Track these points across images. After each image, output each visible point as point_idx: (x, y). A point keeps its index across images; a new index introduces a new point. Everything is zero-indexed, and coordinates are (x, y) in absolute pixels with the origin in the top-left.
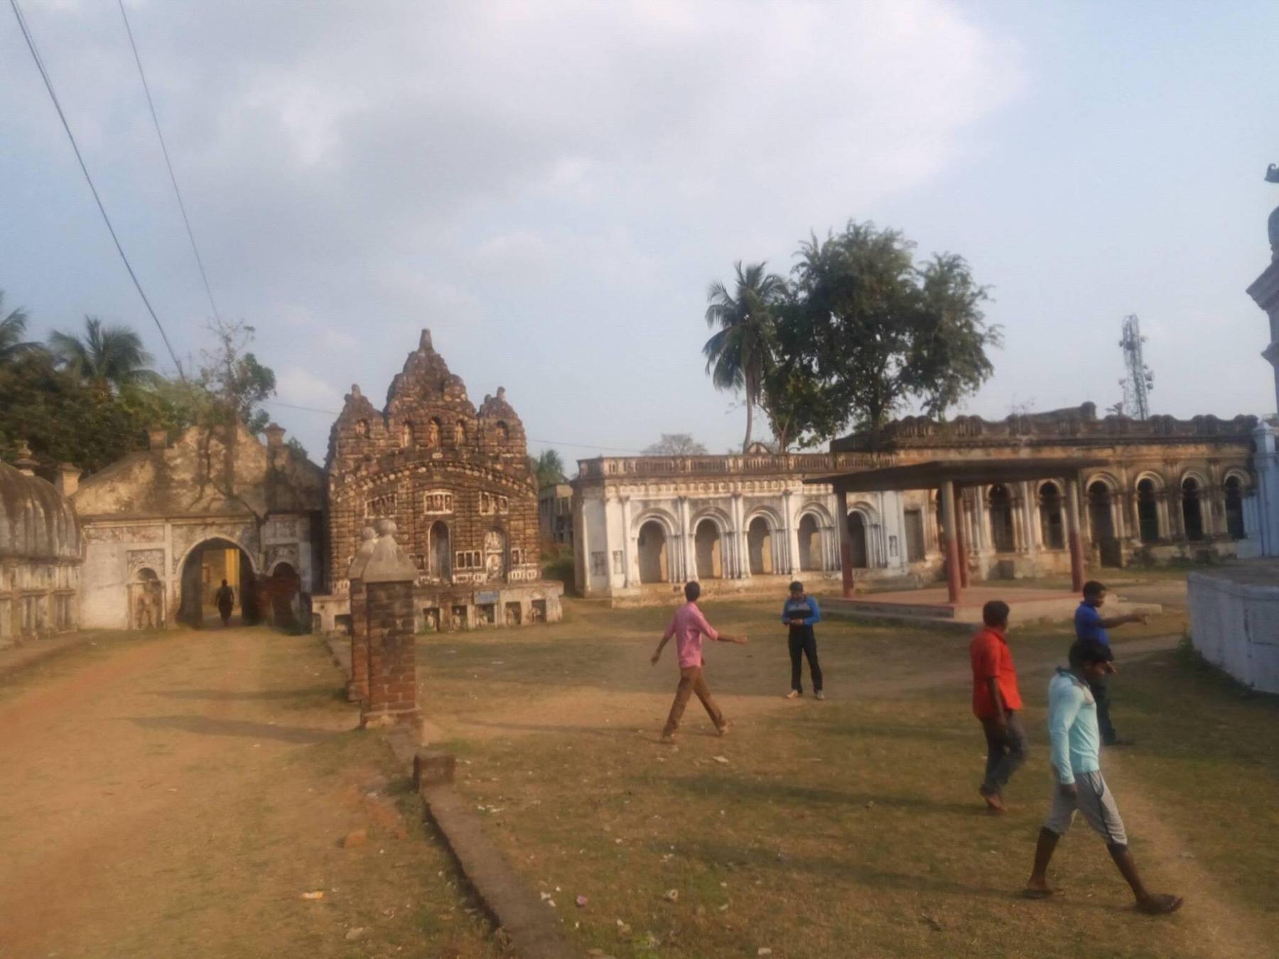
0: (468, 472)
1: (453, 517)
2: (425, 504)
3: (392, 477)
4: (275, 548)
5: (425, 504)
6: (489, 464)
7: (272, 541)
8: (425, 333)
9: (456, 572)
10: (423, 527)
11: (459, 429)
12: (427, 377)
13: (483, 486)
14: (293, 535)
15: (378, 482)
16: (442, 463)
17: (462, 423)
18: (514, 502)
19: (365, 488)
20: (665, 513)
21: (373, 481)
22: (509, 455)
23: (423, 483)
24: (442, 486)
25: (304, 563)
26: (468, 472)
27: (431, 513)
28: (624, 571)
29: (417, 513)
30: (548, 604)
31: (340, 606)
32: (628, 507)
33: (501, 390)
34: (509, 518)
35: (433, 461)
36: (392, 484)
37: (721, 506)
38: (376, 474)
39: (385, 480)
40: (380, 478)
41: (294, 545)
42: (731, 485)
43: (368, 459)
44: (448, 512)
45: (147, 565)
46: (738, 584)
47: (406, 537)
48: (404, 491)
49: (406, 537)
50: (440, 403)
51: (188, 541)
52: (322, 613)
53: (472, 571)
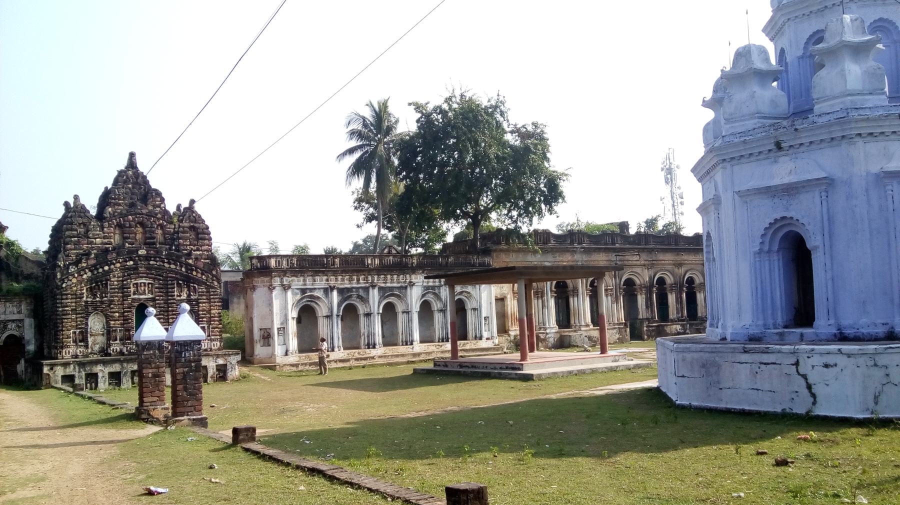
0: (166, 265)
1: (153, 300)
2: (132, 289)
3: (106, 268)
5: (132, 289)
8: (132, 155)
11: (159, 232)
12: (132, 190)
13: (178, 276)
14: (19, 312)
16: (147, 258)
18: (203, 289)
19: (85, 276)
20: (318, 298)
21: (90, 271)
25: (29, 333)
26: (166, 265)
27: (136, 296)
28: (285, 343)
29: (125, 296)
30: (229, 367)
31: (65, 368)
32: (289, 293)
33: (192, 202)
35: (139, 256)
37: (361, 293)
38: (94, 266)
39: (101, 270)
40: (97, 269)
41: (21, 321)
42: (370, 278)
43: (87, 254)
44: (150, 296)
46: (373, 352)
50: (144, 211)
52: (51, 373)
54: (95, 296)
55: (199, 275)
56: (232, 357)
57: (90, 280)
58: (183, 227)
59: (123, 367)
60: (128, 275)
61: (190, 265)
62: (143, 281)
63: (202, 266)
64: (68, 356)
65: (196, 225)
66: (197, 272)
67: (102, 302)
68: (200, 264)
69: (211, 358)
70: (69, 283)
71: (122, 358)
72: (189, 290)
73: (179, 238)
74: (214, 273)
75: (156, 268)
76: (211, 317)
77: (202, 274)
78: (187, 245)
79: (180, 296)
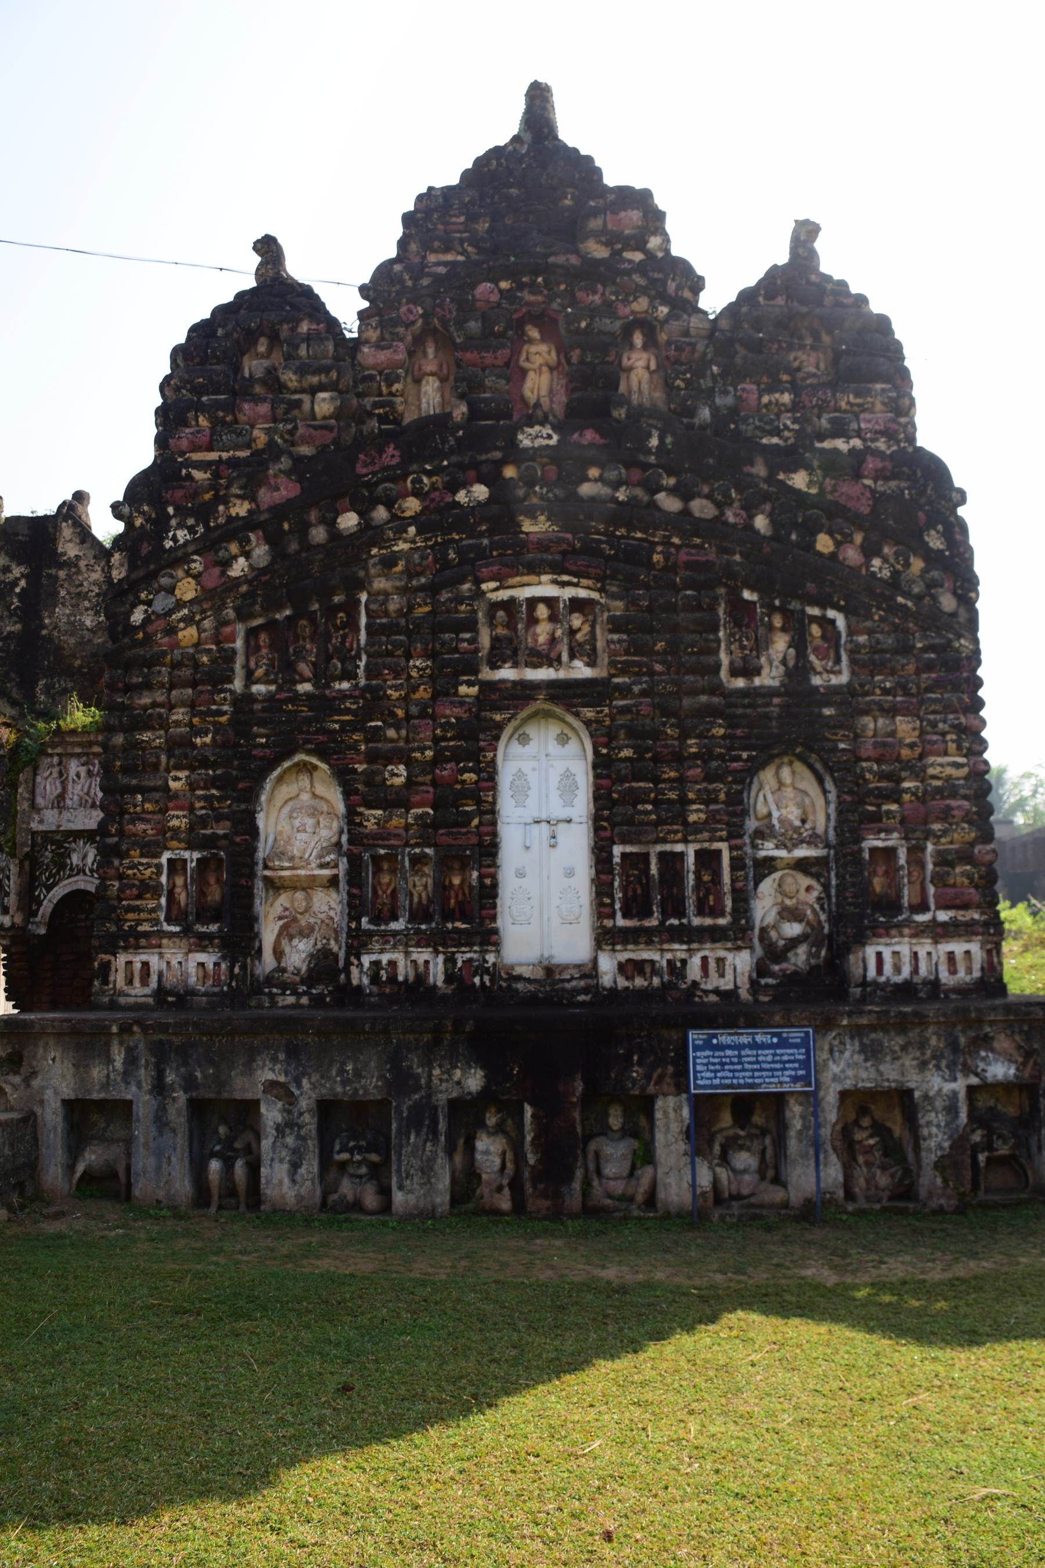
0: (670, 504)
2: (485, 641)
3: (349, 521)
4: (62, 841)
6: (760, 469)
7: (50, 820)
8: (538, 98)
12: (529, 227)
17: (648, 326)
19: (239, 567)
22: (841, 444)
24: (558, 561)
26: (670, 504)
27: (507, 673)
33: (805, 235)
34: (848, 700)
39: (319, 534)
40: (303, 529)
44: (581, 670)
47: (398, 775)
49: (398, 775)
55: (852, 555)
60: (463, 560)
62: (544, 588)
67: (324, 704)
68: (855, 494)
70: (162, 602)
72: (799, 643)
74: (935, 541)
76: (922, 798)
77: (870, 550)
79: (749, 671)
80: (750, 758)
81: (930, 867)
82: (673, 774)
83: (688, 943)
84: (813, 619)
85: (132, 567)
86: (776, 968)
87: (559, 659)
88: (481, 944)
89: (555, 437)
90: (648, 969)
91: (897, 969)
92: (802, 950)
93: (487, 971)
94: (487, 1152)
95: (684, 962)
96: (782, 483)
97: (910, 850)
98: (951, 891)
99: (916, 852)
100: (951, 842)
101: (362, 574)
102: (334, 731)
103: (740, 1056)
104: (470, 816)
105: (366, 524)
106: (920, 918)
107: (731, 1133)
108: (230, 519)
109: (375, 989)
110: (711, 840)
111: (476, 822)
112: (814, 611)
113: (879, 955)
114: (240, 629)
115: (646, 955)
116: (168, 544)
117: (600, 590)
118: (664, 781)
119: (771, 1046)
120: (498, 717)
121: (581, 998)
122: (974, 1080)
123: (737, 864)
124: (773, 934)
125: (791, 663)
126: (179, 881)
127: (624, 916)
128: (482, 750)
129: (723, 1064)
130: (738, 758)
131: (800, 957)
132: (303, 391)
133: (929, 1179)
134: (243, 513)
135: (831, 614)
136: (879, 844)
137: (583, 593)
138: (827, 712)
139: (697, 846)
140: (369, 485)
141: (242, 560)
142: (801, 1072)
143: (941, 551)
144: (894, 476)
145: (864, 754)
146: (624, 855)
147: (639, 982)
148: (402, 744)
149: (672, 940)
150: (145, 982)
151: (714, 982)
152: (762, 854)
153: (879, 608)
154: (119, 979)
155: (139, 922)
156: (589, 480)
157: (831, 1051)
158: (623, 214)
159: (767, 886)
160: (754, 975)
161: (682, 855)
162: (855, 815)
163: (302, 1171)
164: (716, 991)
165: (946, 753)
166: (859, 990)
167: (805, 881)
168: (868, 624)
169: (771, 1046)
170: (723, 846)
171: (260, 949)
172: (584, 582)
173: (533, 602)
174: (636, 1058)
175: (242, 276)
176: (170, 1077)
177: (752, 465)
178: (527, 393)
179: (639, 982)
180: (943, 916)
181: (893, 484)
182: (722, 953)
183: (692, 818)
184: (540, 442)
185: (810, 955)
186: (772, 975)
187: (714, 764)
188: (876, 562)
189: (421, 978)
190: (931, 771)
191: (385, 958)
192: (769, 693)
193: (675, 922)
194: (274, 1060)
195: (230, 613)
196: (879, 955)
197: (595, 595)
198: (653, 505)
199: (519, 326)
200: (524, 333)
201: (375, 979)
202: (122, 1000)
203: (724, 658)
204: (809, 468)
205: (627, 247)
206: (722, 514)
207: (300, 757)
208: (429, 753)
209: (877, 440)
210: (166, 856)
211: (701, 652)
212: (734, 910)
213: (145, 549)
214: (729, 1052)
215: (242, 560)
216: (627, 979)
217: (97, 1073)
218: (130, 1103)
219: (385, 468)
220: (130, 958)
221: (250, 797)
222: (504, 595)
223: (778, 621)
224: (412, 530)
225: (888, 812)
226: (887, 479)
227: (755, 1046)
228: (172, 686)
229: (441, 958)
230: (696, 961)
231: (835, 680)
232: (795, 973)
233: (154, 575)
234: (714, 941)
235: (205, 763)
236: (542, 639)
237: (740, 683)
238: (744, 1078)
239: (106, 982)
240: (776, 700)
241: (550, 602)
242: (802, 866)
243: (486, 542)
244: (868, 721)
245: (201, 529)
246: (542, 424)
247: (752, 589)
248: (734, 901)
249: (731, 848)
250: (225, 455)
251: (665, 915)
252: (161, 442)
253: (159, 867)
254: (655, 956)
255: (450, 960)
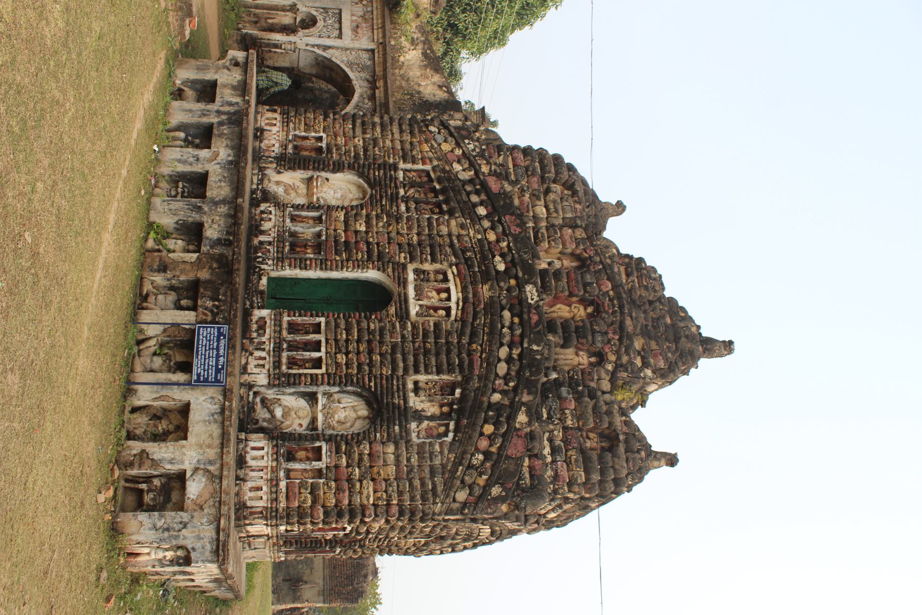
0: (503, 352)
1: (403, 315)
2: (427, 266)
8: (728, 347)
9: (278, 323)
10: (381, 260)
13: (475, 383)
15: (469, 188)
19: (457, 167)
23: (475, 266)
26: (503, 352)
27: (411, 276)
30: (171, 517)
31: (234, 88)
33: (672, 460)
35: (520, 286)
36: (469, 210)
38: (485, 187)
39: (475, 199)
40: (477, 193)
44: (414, 310)
45: (320, 24)
48: (455, 230)
51: (350, 65)
53: (278, 349)
54: (413, 185)
55: (483, 444)
56: (209, 532)
57: (448, 178)
58: (609, 413)
59: (216, 203)
61: (511, 418)
63: (511, 451)
64: (262, 123)
65: (622, 448)
66: (491, 438)
67: (394, 198)
68: (516, 447)
69: (212, 453)
70: (440, 138)
71: (245, 201)
72: (432, 418)
73: (578, 398)
74: (496, 491)
75: (492, 325)
77: (487, 454)
78: (562, 420)
79: (417, 389)
80: (370, 387)
81: (311, 481)
82: (361, 349)
83: (274, 351)
84: (447, 426)
85: (456, 128)
86: (258, 400)
87: (419, 300)
88: (278, 258)
89: (532, 302)
90: (261, 332)
91: (254, 458)
92: (268, 416)
93: (264, 260)
94: (176, 243)
95: (264, 350)
96: (520, 409)
97: (320, 470)
98: (297, 490)
99: (319, 473)
100: (324, 493)
101: (457, 215)
102: (381, 202)
103: (213, 349)
104: (340, 255)
105: (480, 218)
106: (282, 474)
107: (173, 358)
108: (480, 165)
109: (258, 212)
110: (327, 364)
111: (338, 258)
112: (452, 425)
113: (263, 448)
114: (428, 167)
115: (268, 331)
116: (467, 141)
117: (456, 320)
118: (358, 345)
119: (217, 365)
120: (390, 270)
121: (248, 303)
122: (188, 474)
123: (314, 380)
124: (277, 405)
125: (423, 413)
126: (313, 141)
127: (288, 321)
128: (373, 263)
129: (210, 341)
130: (370, 381)
131: (261, 414)
132: (545, 203)
133: (136, 446)
134: (483, 170)
135: (451, 435)
136: (324, 451)
137: (453, 312)
138: (397, 428)
139: (324, 358)
140: (500, 221)
141: (461, 168)
142: (202, 378)
143: (490, 494)
144: (531, 476)
145: (373, 446)
146: (319, 324)
147: (254, 327)
148: (375, 229)
149: (275, 343)
150: (266, 124)
151: (252, 362)
152: (320, 396)
153: (455, 458)
154: (270, 115)
155: (295, 123)
156: (512, 316)
157: (212, 398)
158: (661, 358)
159: (302, 403)
160: (255, 389)
161: (319, 351)
162: (341, 442)
163: (176, 163)
164: (247, 363)
165: (375, 492)
166: (243, 437)
167: (305, 423)
168: (446, 451)
169: (217, 365)
170: (323, 370)
171: (279, 173)
172: (460, 312)
173: (448, 290)
174: (217, 303)
175: (606, 195)
176: (224, 117)
177: (528, 394)
178: (559, 306)
179: (254, 327)
180: (283, 484)
181: (527, 475)
182: (267, 367)
183: (339, 356)
184: (529, 295)
185: (264, 420)
186: (255, 397)
187: (366, 368)
188: (481, 457)
189: (263, 233)
190: (365, 482)
191: (272, 217)
192: (405, 400)
193: (285, 346)
194: (229, 155)
195: (435, 163)
196: (263, 448)
197: (453, 318)
198: (502, 345)
199: (591, 303)
200: (589, 305)
201: (262, 212)
202: (259, 116)
203: (422, 378)
204: (529, 423)
205: (643, 358)
206: (500, 378)
207: (369, 190)
208: (371, 240)
209: (552, 470)
210: (324, 136)
211: (426, 366)
212: (290, 375)
213: (464, 133)
214: (215, 344)
215: (461, 168)
216: (257, 322)
217: (228, 92)
218: (214, 101)
219: (509, 226)
220: (278, 119)
221: (351, 167)
222: (450, 277)
223: (445, 409)
224: (480, 237)
225: (341, 457)
226: (530, 472)
227: (218, 356)
228: (401, 142)
229: (271, 239)
230: (263, 354)
231: (414, 435)
232: (255, 411)
233: (451, 135)
234: (274, 363)
235: (366, 150)
236: (429, 294)
237: (410, 386)
238: (202, 350)
239: (268, 110)
240: (402, 402)
241: (449, 299)
242: (314, 420)
243: (477, 269)
244: (391, 449)
245: (474, 154)
246: (538, 296)
247: (462, 394)
248: (295, 375)
249: (322, 375)
250: (511, 170)
251: (289, 342)
252: (515, 148)
253: (319, 132)
254: (267, 336)
255: (270, 243)
